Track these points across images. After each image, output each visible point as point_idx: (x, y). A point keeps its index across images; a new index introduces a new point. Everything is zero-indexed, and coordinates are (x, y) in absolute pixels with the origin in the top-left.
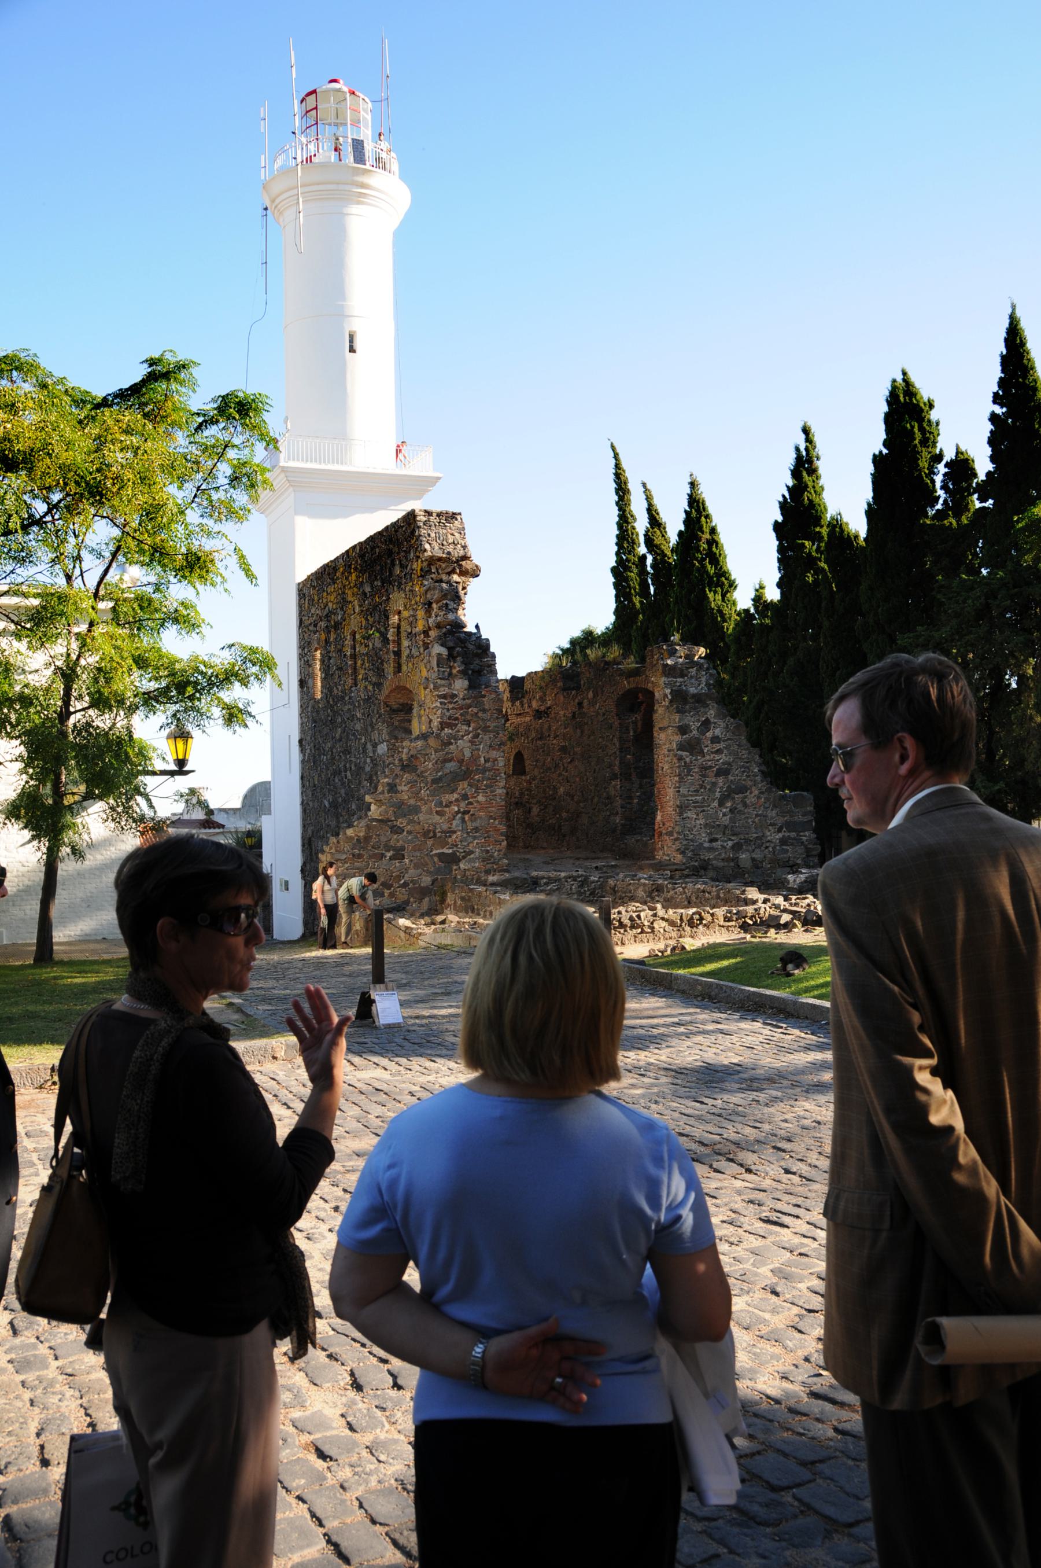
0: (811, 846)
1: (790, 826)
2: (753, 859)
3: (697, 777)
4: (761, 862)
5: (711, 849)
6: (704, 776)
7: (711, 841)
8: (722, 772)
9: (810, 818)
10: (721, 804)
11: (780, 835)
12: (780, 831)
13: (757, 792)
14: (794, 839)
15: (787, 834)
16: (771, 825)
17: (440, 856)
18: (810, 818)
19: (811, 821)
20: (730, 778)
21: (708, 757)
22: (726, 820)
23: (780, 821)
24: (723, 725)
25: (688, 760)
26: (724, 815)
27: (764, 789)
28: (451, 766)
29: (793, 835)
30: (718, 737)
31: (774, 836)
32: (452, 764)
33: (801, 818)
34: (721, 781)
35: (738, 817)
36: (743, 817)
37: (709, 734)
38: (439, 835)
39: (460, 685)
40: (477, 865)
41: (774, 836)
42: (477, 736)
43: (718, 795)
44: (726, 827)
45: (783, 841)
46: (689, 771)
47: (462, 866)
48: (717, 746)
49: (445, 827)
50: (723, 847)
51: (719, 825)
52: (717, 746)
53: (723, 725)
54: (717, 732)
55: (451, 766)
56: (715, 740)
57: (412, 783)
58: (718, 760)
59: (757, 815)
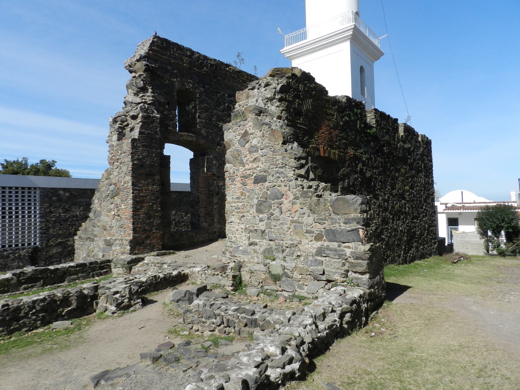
0: (351, 260)
1: (332, 235)
2: (284, 268)
3: (239, 185)
4: (292, 271)
5: (245, 252)
6: (244, 184)
7: (251, 244)
8: (259, 180)
9: (354, 226)
10: (259, 211)
11: (318, 244)
12: (318, 238)
13: (292, 197)
14: (335, 250)
15: (326, 243)
16: (307, 232)
17: (105, 240)
18: (354, 226)
19: (357, 230)
20: (267, 184)
21: (247, 167)
22: (262, 226)
23: (318, 228)
24: (259, 134)
25: (231, 171)
26: (261, 220)
27: (298, 194)
28: (112, 187)
29: (334, 245)
30: (255, 146)
31: (310, 246)
32: (113, 186)
33: (343, 226)
34: (257, 187)
35: (274, 223)
36: (279, 222)
37: (247, 146)
38: (108, 228)
39: (115, 137)
40: (118, 248)
41: (310, 246)
42: (121, 169)
43: (256, 201)
44: (263, 232)
45: (320, 252)
46: (233, 180)
47: (114, 248)
48: (255, 155)
49: (110, 223)
50: (255, 251)
51: (256, 230)
52: (255, 155)
53: (259, 134)
54: (254, 142)
55: (112, 187)
56: (253, 149)
57: (98, 199)
58: (255, 169)
59: (292, 222)
